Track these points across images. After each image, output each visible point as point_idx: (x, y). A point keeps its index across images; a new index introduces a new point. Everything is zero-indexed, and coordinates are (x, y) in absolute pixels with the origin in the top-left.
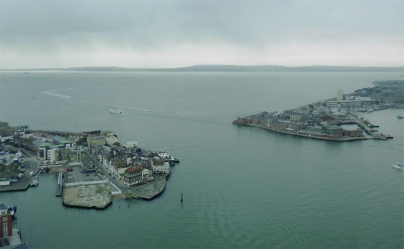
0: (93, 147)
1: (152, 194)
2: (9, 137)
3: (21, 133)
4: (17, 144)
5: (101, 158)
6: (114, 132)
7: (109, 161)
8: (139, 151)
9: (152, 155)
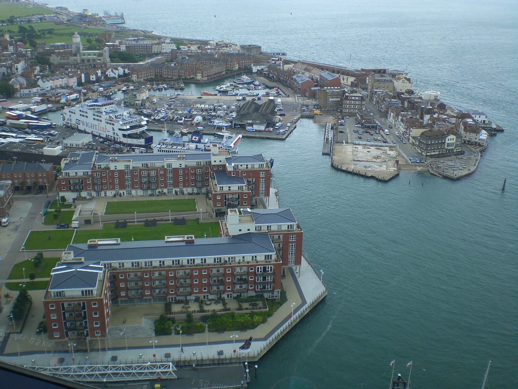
0: (376, 92)
1: (459, 173)
2: (263, 67)
3: (278, 62)
4: (273, 77)
6: (407, 74)
7: (397, 115)
8: (442, 107)
9: (463, 116)
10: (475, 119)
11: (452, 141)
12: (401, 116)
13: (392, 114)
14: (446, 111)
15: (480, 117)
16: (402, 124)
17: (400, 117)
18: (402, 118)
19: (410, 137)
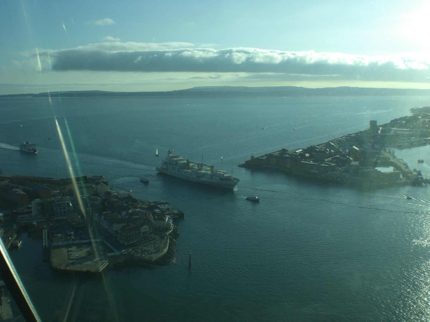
5: (91, 211)
10: (161, 208)
11: (146, 230)
12: (103, 215)
13: (96, 214)
14: (138, 204)
15: (164, 206)
16: (105, 222)
17: (103, 217)
18: (104, 216)
19: (113, 232)
